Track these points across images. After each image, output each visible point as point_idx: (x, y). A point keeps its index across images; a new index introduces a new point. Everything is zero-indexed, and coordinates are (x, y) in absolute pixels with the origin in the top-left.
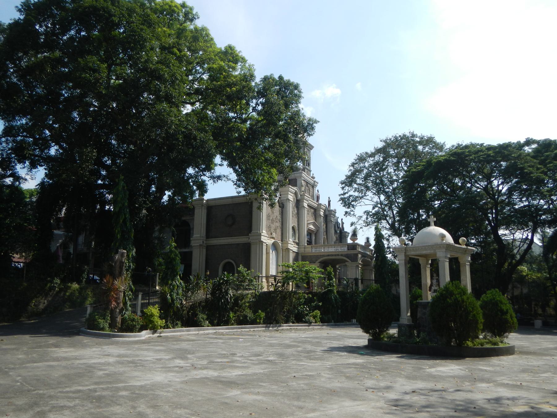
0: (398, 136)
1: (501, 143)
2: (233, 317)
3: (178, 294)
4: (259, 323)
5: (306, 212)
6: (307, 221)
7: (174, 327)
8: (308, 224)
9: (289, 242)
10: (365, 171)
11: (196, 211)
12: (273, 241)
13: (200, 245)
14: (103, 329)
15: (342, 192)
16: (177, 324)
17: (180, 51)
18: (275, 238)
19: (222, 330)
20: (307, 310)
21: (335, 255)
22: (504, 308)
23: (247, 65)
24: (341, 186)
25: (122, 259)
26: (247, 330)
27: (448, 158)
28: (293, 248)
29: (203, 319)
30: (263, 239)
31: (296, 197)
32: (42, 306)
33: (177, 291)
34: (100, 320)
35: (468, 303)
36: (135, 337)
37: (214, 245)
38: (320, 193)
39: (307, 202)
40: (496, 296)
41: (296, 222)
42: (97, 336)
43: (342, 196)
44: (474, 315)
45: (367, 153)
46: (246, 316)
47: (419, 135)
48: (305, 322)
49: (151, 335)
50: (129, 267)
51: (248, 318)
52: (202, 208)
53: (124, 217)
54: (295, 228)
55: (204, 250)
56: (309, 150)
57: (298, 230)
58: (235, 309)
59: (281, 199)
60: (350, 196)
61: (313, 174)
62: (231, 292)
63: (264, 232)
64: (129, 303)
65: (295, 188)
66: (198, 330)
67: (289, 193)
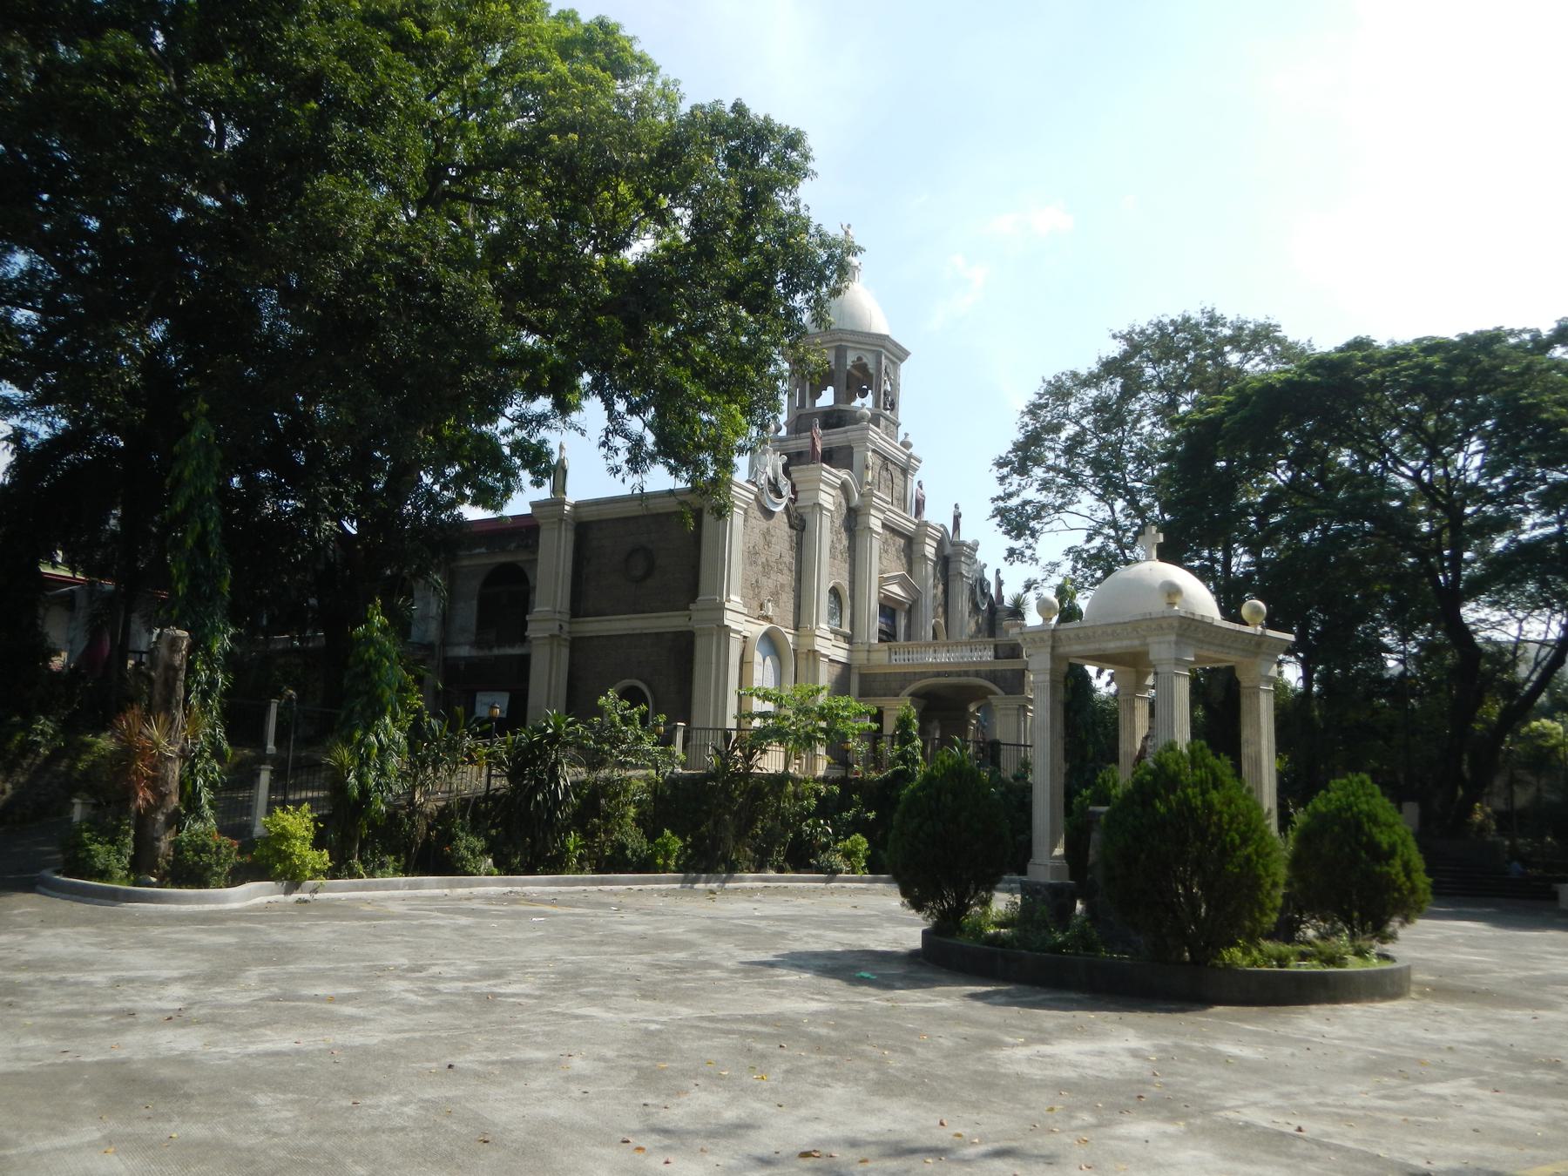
0: (1166, 320)
1: (1471, 332)
2: (576, 847)
3: (383, 772)
4: (665, 869)
5: (876, 544)
6: (882, 572)
7: (371, 874)
8: (884, 581)
9: (817, 632)
10: (1070, 430)
11: (544, 537)
12: (766, 626)
13: (552, 636)
14: (104, 874)
15: (999, 491)
16: (382, 865)
17: (424, 26)
18: (775, 619)
19: (535, 886)
20: (826, 834)
21: (959, 674)
22: (1383, 839)
23: (658, 83)
24: (996, 472)
25: (171, 658)
26: (621, 889)
27: (1296, 378)
28: (831, 648)
29: (473, 852)
30: (730, 619)
31: (848, 500)
33: (382, 763)
34: (96, 846)
35: (1226, 818)
36: (216, 900)
37: (591, 637)
38: (926, 491)
39: (881, 516)
40: (1358, 798)
41: (846, 575)
43: (1001, 504)
44: (1248, 859)
45: (1075, 375)
46: (623, 847)
47: (1231, 317)
48: (819, 870)
49: (281, 897)
50: (212, 683)
51: (629, 853)
53: (199, 527)
55: (565, 653)
56: (894, 363)
57: (852, 597)
58: (593, 825)
60: (1026, 503)
61: (906, 435)
62: (570, 774)
63: (735, 600)
64: (206, 796)
65: (844, 474)
66: (451, 886)
67: (822, 486)
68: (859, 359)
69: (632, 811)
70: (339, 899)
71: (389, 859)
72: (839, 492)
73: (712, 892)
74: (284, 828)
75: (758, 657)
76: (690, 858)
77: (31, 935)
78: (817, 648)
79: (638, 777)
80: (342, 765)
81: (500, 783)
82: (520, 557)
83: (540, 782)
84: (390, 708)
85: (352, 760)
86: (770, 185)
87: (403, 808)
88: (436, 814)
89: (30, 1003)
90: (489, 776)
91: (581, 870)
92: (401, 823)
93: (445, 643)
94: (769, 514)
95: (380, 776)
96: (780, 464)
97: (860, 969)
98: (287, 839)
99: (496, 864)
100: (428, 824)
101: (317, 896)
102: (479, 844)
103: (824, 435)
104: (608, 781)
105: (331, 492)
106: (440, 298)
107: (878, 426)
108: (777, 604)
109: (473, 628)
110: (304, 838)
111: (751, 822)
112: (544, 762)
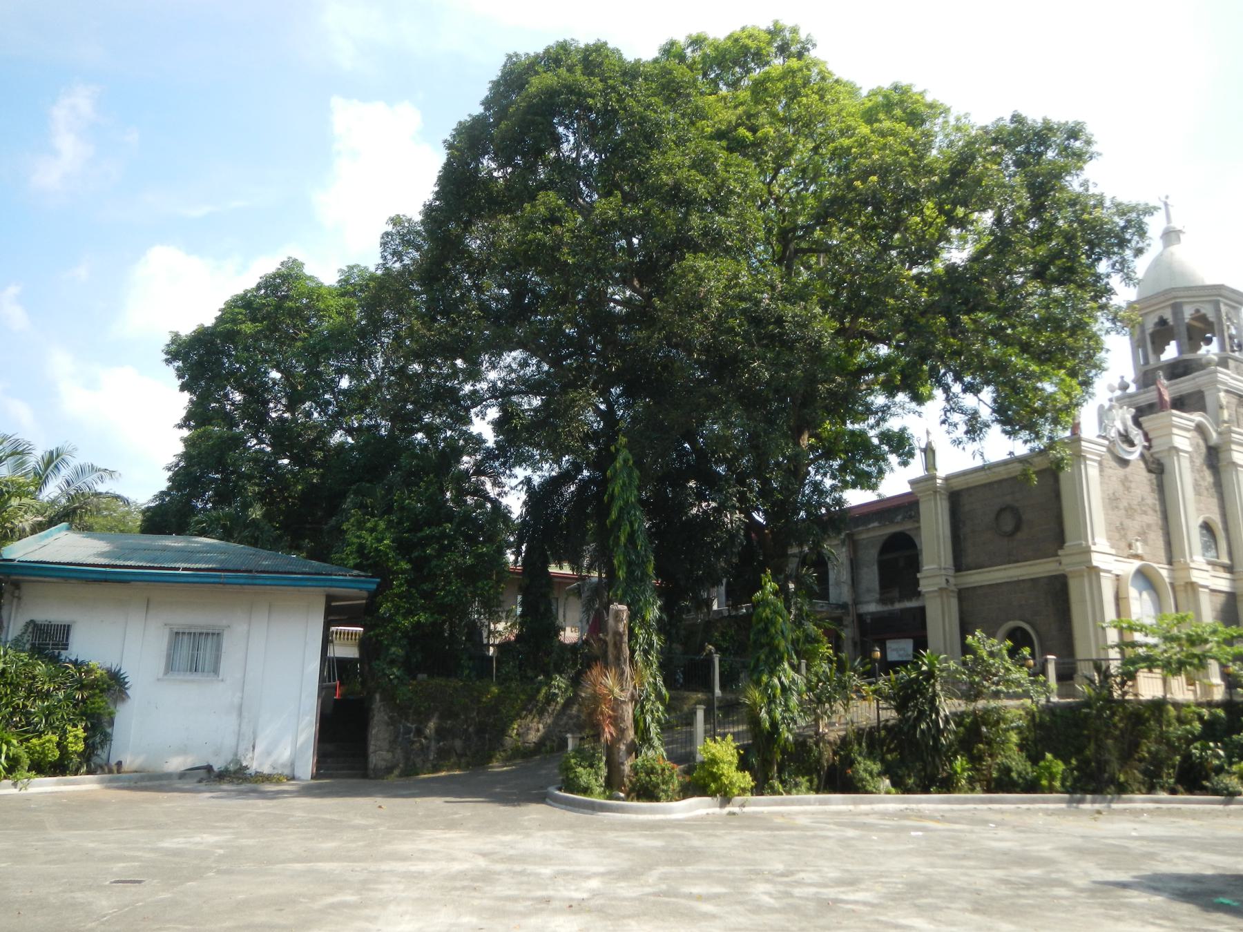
2: (963, 770)
3: (787, 709)
4: (1051, 790)
7: (789, 793)
9: (1192, 565)
11: (923, 508)
12: (1137, 564)
13: (941, 589)
14: (586, 790)
16: (797, 785)
17: (754, 130)
18: (1145, 557)
19: (930, 804)
20: (1218, 757)
23: (952, 122)
25: (617, 626)
26: (1010, 806)
29: (871, 774)
30: (1097, 560)
32: (533, 737)
33: (786, 700)
34: (580, 769)
36: (663, 811)
37: (975, 588)
42: (570, 805)
46: (1008, 770)
48: (1215, 792)
49: (717, 810)
50: (651, 645)
51: (1014, 775)
52: (935, 500)
53: (628, 528)
54: (1214, 527)
55: (954, 602)
57: (1226, 529)
58: (979, 750)
59: (1152, 450)
62: (948, 706)
64: (654, 730)
65: (1197, 417)
66: (855, 803)
67: (1175, 431)
68: (1197, 311)
69: (1014, 738)
70: (763, 812)
71: (803, 780)
72: (1195, 434)
73: (1099, 812)
74: (713, 755)
75: (1133, 592)
76: (1076, 780)
77: (528, 835)
78: (1194, 579)
79: (1014, 709)
80: (755, 703)
81: (890, 715)
82: (906, 527)
83: (922, 713)
84: (786, 656)
85: (762, 698)
86: (1057, 174)
87: (811, 737)
88: (839, 742)
89: (489, 888)
90: (878, 708)
91: (973, 790)
92: (810, 750)
93: (856, 602)
94: (1124, 463)
95: (784, 711)
96: (1129, 417)
97: (1222, 893)
98: (717, 763)
99: (894, 784)
100: (833, 750)
101: (746, 809)
102: (876, 767)
103: (1171, 385)
104: (987, 711)
105: (739, 492)
106: (783, 327)
107: (1227, 367)
108: (1145, 542)
109: (877, 588)
110: (731, 763)
111: (1135, 746)
112: (923, 695)
